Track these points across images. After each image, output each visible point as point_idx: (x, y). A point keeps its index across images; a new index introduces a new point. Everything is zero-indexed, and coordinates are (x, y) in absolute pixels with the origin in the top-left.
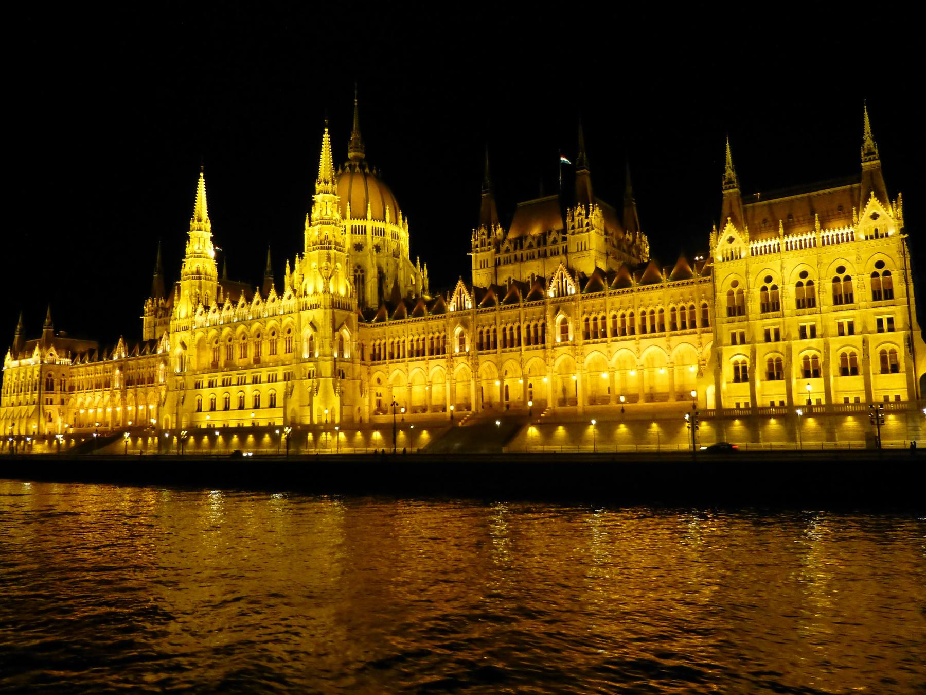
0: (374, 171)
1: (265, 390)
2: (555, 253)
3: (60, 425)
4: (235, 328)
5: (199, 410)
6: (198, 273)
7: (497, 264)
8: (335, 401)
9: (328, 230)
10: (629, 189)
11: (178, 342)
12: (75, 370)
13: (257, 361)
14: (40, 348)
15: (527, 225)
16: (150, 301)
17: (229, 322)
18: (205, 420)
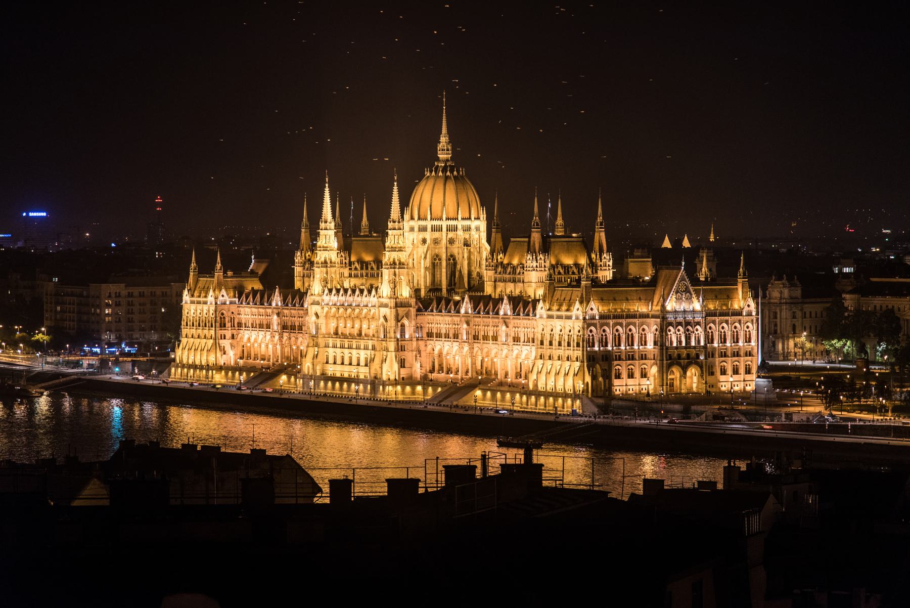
0: (455, 173)
1: (363, 355)
2: (519, 281)
3: (231, 357)
4: (346, 310)
5: (327, 363)
6: (326, 262)
7: (495, 281)
8: (396, 366)
9: (394, 255)
10: (600, 219)
11: (313, 312)
12: (242, 309)
13: (360, 334)
14: (214, 291)
15: (512, 257)
16: (299, 253)
17: (343, 305)
18: (331, 370)
